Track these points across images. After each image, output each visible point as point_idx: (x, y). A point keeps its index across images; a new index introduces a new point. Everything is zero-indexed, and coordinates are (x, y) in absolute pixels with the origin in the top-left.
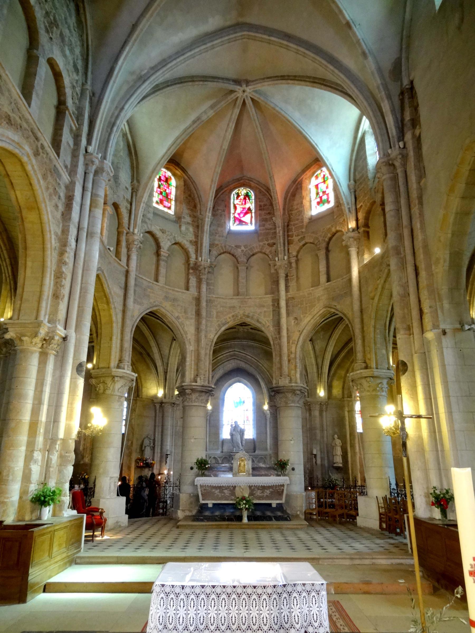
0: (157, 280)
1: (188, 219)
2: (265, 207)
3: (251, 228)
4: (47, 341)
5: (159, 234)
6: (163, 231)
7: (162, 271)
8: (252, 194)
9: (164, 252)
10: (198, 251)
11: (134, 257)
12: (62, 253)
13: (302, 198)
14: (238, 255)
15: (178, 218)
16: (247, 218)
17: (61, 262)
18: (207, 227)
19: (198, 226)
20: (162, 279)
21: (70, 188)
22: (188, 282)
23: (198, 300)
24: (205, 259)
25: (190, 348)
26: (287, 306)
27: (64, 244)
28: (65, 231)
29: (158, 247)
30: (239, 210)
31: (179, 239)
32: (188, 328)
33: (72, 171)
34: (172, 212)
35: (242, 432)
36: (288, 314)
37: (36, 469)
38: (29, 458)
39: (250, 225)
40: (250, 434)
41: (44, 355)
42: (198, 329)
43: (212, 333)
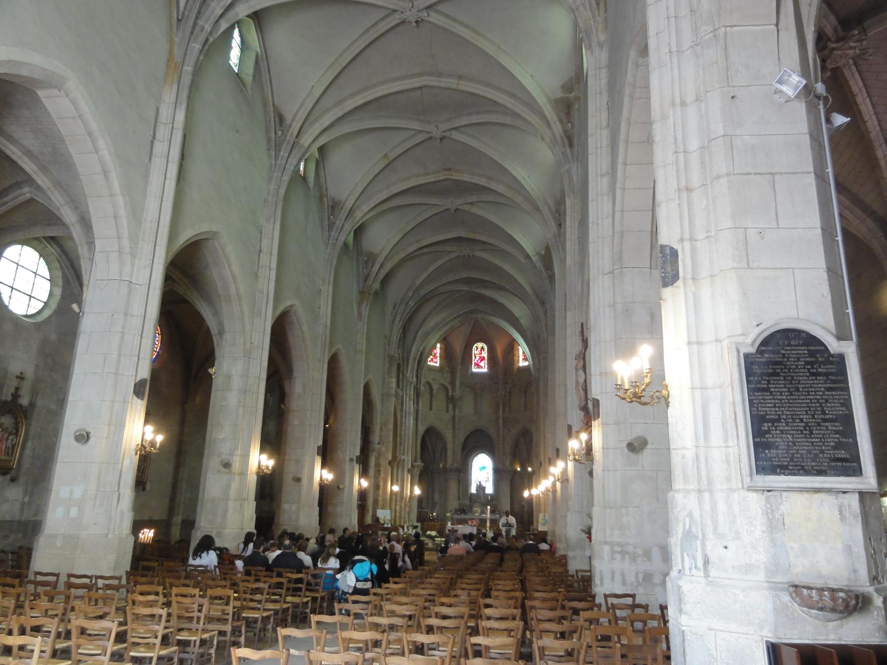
0: (431, 409)
1: (447, 369)
2: (492, 359)
3: (485, 370)
4: (399, 462)
5: (431, 382)
6: (434, 380)
7: (434, 403)
8: (486, 347)
9: (434, 392)
10: (454, 390)
11: (420, 402)
12: (401, 426)
13: (514, 355)
14: (476, 385)
15: (441, 369)
16: (482, 364)
17: (401, 430)
18: (458, 375)
19: (453, 372)
20: (434, 408)
21: (402, 396)
22: (448, 407)
23: (453, 418)
24: (457, 393)
25: (450, 446)
26: (503, 422)
27: (402, 422)
28: (401, 416)
29: (431, 390)
30: (477, 358)
31: (443, 382)
32: (448, 435)
33: (402, 390)
34: (438, 365)
35: (484, 489)
36: (504, 426)
37: (398, 508)
38: (396, 504)
39: (484, 368)
40: (489, 490)
41: (398, 467)
42: (454, 436)
43: (461, 438)
